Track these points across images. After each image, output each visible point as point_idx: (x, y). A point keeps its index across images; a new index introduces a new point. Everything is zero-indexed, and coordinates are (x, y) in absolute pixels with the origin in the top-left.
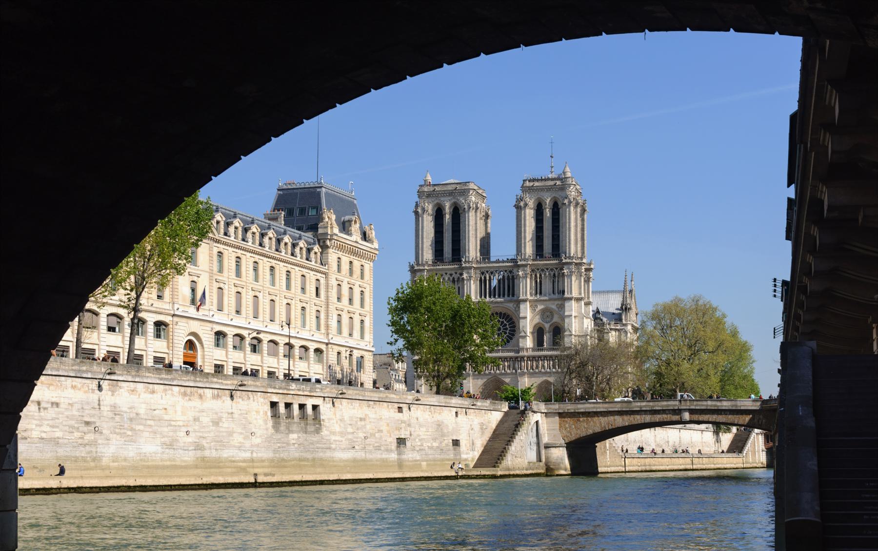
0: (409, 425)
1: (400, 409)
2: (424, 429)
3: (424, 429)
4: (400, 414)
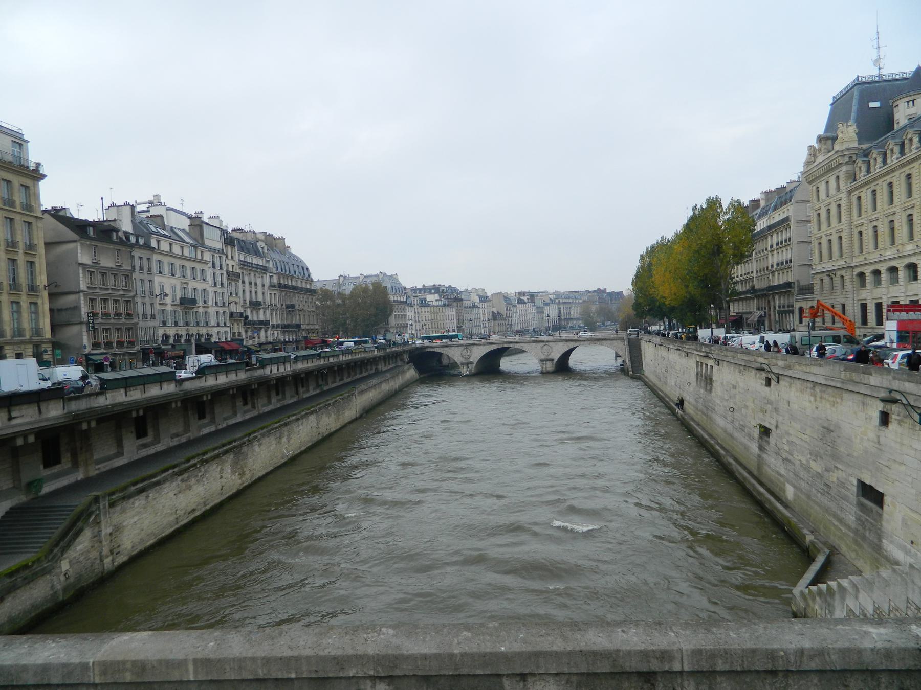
0: (776, 410)
1: (768, 382)
2: (798, 426)
3: (798, 426)
4: (767, 389)
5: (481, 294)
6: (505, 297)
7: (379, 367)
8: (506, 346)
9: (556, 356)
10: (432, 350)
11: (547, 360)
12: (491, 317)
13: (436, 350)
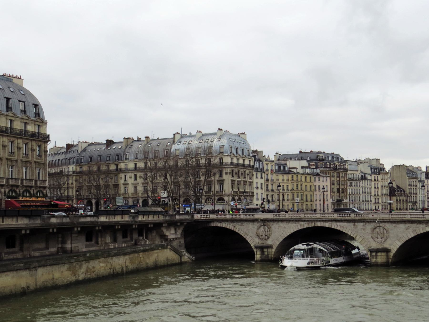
5: (375, 165)
6: (408, 170)
7: (68, 246)
8: (319, 224)
9: (394, 245)
10: (219, 225)
11: (377, 251)
12: (387, 191)
13: (224, 225)
